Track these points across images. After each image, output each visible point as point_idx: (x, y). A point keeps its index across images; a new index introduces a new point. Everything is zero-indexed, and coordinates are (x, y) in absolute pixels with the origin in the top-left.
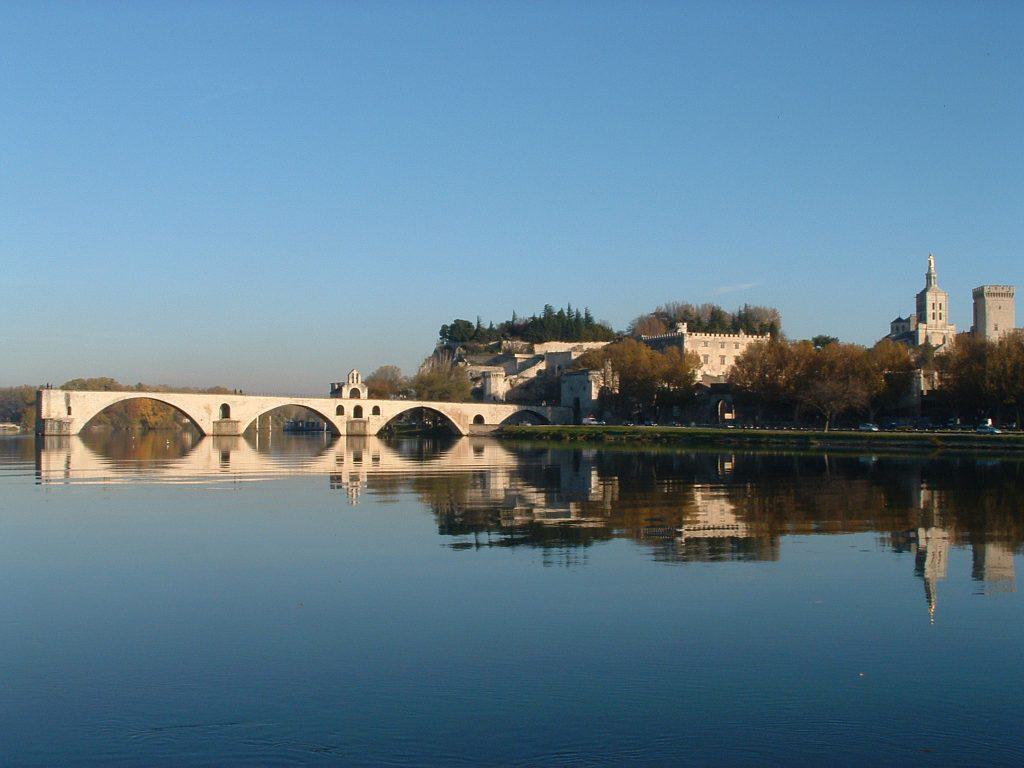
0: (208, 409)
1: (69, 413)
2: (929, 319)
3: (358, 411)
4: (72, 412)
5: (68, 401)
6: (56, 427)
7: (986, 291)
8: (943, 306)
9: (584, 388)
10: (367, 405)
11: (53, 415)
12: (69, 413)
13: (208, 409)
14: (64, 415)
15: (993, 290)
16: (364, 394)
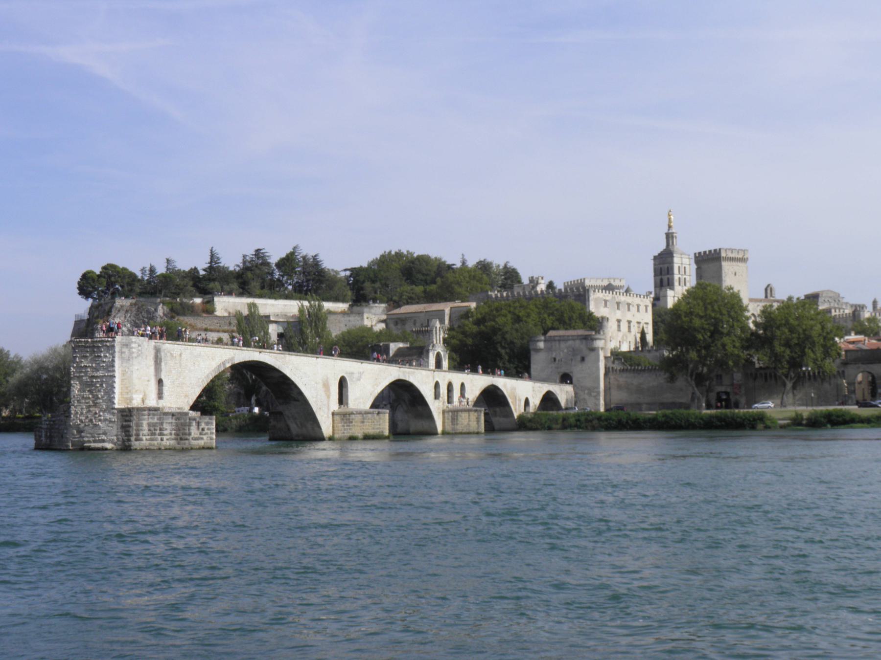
0: (326, 386)
1: (160, 396)
2: (676, 283)
3: (450, 387)
4: (166, 389)
5: (158, 361)
6: (168, 428)
7: (723, 254)
8: (687, 270)
9: (583, 359)
10: (457, 378)
11: (136, 402)
12: (160, 396)
13: (326, 386)
14: (152, 402)
15: (730, 255)
16: (445, 364)
